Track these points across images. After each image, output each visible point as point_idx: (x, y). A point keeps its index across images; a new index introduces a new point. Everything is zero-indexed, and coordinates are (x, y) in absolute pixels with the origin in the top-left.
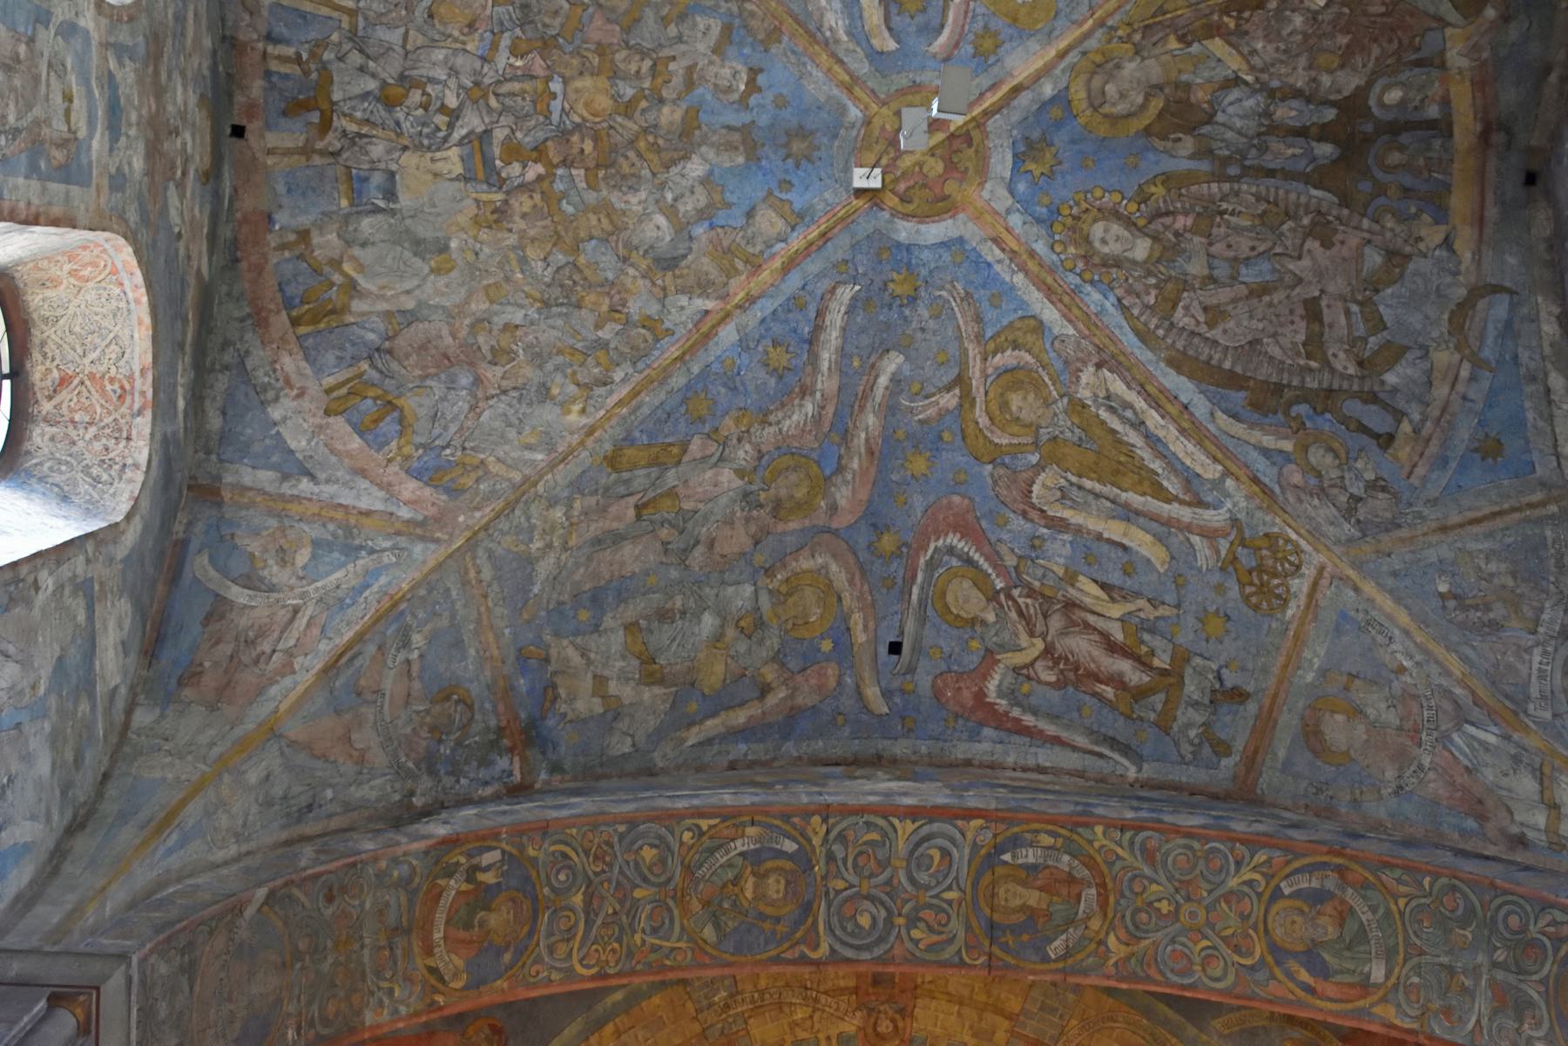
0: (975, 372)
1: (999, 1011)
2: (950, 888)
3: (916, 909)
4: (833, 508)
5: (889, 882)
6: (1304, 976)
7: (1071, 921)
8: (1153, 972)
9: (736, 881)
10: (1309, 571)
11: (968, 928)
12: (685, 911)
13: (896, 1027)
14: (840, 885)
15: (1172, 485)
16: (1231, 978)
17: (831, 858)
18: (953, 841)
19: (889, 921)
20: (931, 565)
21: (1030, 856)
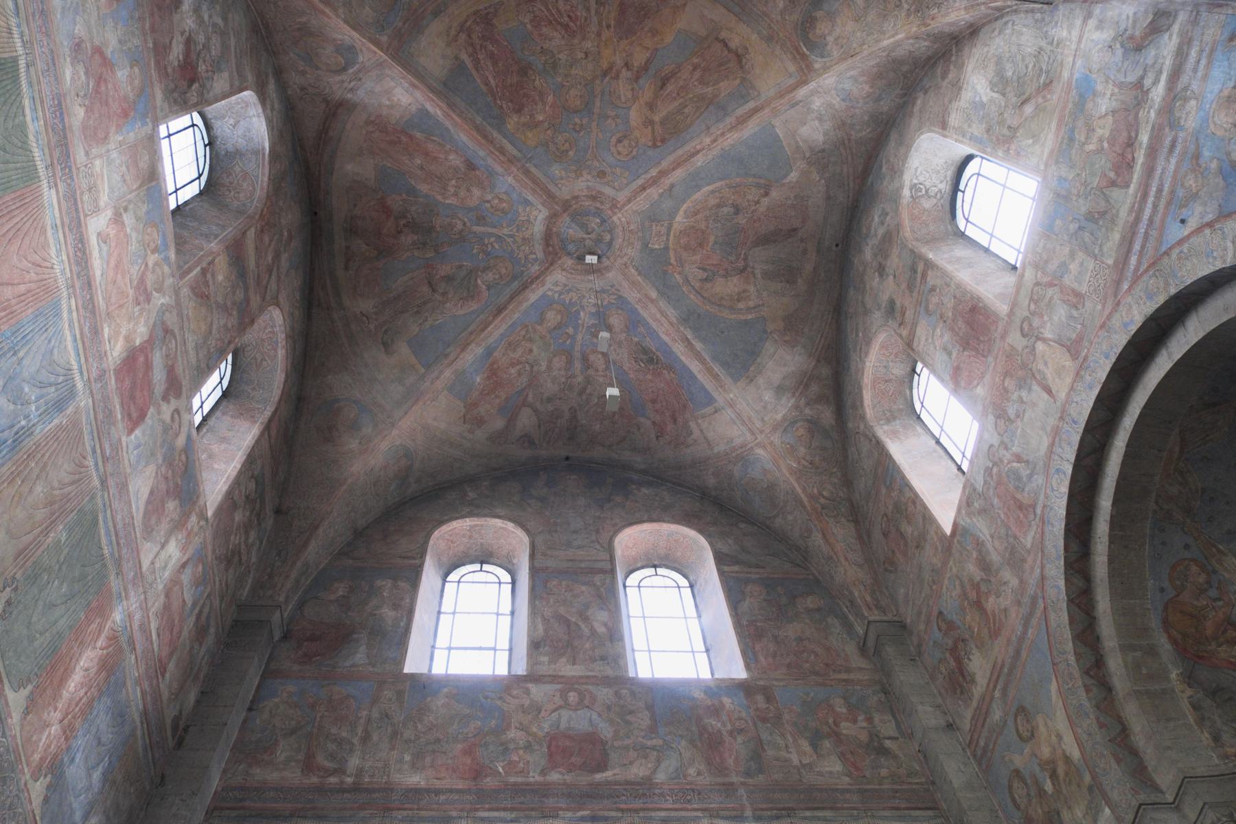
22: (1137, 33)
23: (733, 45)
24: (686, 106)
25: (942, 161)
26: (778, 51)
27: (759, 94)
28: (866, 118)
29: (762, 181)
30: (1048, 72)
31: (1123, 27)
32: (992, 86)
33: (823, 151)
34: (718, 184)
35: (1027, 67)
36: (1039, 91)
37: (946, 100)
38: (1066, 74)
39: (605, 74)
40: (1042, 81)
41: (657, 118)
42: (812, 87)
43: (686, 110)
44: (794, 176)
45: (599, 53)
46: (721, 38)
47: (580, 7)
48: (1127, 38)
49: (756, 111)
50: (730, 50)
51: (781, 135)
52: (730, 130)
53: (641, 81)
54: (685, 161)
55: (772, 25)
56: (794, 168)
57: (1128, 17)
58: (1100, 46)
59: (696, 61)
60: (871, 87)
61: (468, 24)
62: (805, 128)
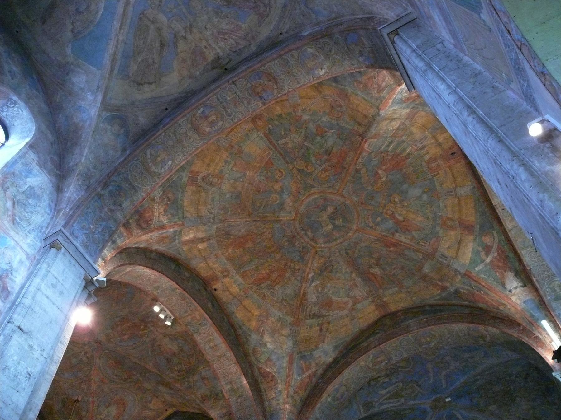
0: (419, 389)
4: (432, 364)
6: (336, 387)
7: (371, 361)
10: (362, 413)
15: (385, 401)
19: (401, 344)
20: (410, 363)
21: (383, 364)
22: (7, 280)
23: (146, 86)
24: (144, 44)
25: (16, 124)
26: (126, 102)
27: (117, 79)
28: (64, 105)
29: (81, 36)
30: (18, 223)
31: (14, 273)
32: (31, 188)
33: (67, 74)
34: (98, 18)
35: (27, 212)
36: (14, 214)
37: (41, 155)
38: (12, 233)
39: (191, 26)
40: (17, 218)
41: (152, 26)
42: (98, 102)
43: (142, 42)
44: (69, 50)
45: (201, 33)
46: (154, 84)
47: (224, 46)
48: (8, 273)
49: (112, 71)
50: (145, 83)
51: (91, 67)
52: (115, 53)
53: (173, 36)
54: (123, 19)
55: (137, 109)
56: (72, 55)
57: (16, 278)
58: (13, 258)
59: (156, 66)
60: (74, 123)
61: (268, 9)
62: (84, 80)
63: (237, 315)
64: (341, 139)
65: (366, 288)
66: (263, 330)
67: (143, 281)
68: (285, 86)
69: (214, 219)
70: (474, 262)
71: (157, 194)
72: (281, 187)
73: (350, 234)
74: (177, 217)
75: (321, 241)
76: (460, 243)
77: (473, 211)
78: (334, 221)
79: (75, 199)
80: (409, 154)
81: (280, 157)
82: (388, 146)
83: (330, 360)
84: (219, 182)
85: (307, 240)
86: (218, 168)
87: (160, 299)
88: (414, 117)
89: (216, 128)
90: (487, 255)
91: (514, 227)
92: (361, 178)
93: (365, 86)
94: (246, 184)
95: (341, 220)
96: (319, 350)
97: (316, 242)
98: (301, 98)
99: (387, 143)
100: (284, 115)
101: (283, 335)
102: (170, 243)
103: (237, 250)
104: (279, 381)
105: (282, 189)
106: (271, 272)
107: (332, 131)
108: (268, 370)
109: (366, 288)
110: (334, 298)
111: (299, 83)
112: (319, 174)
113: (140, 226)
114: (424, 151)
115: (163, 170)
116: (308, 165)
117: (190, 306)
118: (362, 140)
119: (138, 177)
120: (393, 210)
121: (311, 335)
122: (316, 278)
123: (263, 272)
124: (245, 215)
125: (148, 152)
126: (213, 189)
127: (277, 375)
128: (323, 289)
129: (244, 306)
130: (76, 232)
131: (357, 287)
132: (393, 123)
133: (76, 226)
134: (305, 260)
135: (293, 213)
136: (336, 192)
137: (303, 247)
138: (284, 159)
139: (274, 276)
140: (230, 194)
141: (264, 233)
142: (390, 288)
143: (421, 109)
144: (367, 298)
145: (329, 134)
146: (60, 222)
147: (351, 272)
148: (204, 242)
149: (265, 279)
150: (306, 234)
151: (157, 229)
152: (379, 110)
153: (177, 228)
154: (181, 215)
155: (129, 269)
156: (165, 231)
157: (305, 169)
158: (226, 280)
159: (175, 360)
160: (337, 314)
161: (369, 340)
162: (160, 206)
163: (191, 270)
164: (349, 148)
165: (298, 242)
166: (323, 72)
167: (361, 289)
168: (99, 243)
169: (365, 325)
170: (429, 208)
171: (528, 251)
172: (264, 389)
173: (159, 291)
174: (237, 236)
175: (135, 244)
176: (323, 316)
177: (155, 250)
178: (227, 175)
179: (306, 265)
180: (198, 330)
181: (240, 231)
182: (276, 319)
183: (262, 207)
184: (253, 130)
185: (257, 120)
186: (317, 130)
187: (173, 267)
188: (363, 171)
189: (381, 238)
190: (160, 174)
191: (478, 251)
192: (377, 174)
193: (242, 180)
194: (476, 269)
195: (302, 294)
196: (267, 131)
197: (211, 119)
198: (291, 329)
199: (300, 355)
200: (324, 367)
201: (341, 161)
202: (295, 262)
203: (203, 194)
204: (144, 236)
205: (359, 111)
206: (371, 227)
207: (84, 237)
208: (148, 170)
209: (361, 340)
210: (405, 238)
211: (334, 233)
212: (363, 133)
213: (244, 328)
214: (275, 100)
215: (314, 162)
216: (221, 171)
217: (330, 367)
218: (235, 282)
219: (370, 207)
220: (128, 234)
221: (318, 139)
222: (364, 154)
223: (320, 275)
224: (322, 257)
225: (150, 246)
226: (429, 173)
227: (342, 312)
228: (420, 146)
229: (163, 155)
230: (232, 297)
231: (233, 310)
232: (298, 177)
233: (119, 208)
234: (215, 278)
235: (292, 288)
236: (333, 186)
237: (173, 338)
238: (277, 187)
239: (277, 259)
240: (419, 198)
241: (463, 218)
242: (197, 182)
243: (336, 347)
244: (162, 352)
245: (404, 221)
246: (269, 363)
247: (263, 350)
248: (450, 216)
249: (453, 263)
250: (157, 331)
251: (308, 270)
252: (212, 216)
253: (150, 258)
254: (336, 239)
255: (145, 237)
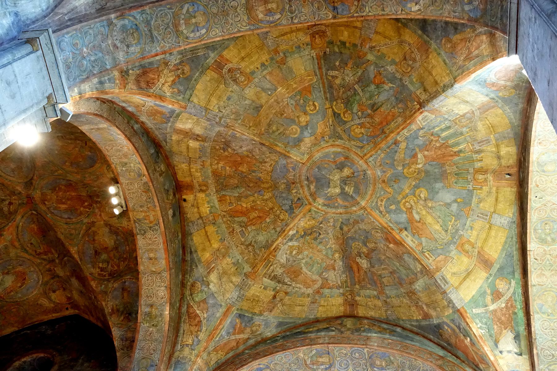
1: (324, 306)
2: (339, 360)
3: (346, 356)
5: (353, 361)
6: (261, 366)
7: (312, 357)
8: (292, 353)
9: (387, 366)
11: (334, 353)
12: (398, 364)
13: (347, 297)
14: (363, 361)
16: (276, 359)
17: (366, 366)
18: (339, 368)
63: (194, 238)
64: (397, 99)
65: (344, 276)
66: (213, 267)
67: (112, 149)
68: (367, 8)
69: (221, 118)
70: (475, 302)
71: (174, 60)
72: (306, 122)
73: (354, 208)
74: (182, 96)
75: (320, 201)
76: (469, 274)
77: (500, 248)
78: (343, 186)
79: (81, 12)
80: (460, 151)
81: (322, 89)
82: (442, 130)
83: (269, 334)
84: (246, 82)
85: (307, 193)
86: (252, 67)
87: (121, 178)
88: (487, 110)
89: (271, 19)
90: (493, 301)
91: (539, 285)
92: (396, 152)
93: (454, 47)
94: (273, 100)
95: (352, 189)
96: (262, 318)
97: (314, 200)
98: (377, 33)
99: (443, 126)
100: (347, 45)
101: (232, 282)
102: (162, 123)
103: (228, 168)
104: (204, 329)
105: (307, 125)
106: (253, 209)
107: (392, 85)
108: (198, 312)
109: (344, 276)
110: (304, 270)
111: (383, 10)
112: (355, 127)
113: (138, 81)
114: (478, 156)
115: (192, 35)
116: (347, 111)
117: (150, 202)
118: (419, 109)
119: (162, 27)
120: (413, 204)
121: (261, 297)
122: (295, 238)
123: (245, 205)
124: (255, 132)
125: (186, 7)
126: (235, 86)
127: (204, 322)
128: (298, 253)
129: (206, 232)
130: (64, 44)
131: (334, 269)
132: (462, 106)
133: (67, 38)
134: (294, 213)
135: (306, 157)
136: (362, 155)
137: (299, 199)
138: (325, 92)
139: (254, 215)
140: (251, 102)
141: (265, 162)
142: (369, 289)
143: (500, 106)
144: (339, 287)
145: (386, 87)
146: (51, 25)
147: (336, 251)
148: (197, 140)
149: (244, 213)
150: (308, 186)
151: (155, 97)
152: (455, 81)
153: (176, 107)
154: (187, 97)
155: (104, 125)
156: (162, 104)
157: (342, 115)
158: (201, 195)
159: (104, 256)
160: (300, 288)
161: (319, 334)
162: (170, 74)
163: (170, 166)
164: (400, 113)
165: (296, 191)
166: (416, 8)
167: (338, 275)
168: (85, 71)
169: (323, 316)
170: (453, 221)
171: (543, 318)
172: (184, 331)
173: (124, 169)
174: (236, 152)
175: (124, 102)
176: (284, 283)
177: (142, 122)
178: (256, 80)
179: (293, 219)
180: (145, 232)
181: (241, 147)
182: (233, 261)
183: (277, 133)
184: (307, 45)
185: (317, 36)
186: (375, 77)
187: (152, 151)
188: (403, 145)
189: (385, 228)
190: (187, 38)
191: (485, 292)
192: (415, 156)
193: (270, 93)
194: (474, 310)
195: (274, 246)
196: (321, 54)
197: (270, 6)
198: (244, 280)
199: (239, 312)
200: (259, 339)
201: (384, 123)
202: (282, 210)
203: (222, 86)
204: (137, 97)
205: (432, 75)
206: (381, 212)
207: (71, 56)
208: (176, 26)
209: (311, 330)
210: (412, 240)
211: (338, 200)
212: (424, 102)
213: (195, 256)
214: (348, 17)
215: (355, 111)
216: (253, 73)
217: (264, 341)
218: (208, 202)
219: (390, 190)
220: (121, 84)
221: (373, 87)
222: (414, 127)
223: (302, 237)
224: (314, 218)
225: (138, 114)
226: (471, 183)
227: (305, 289)
228: (478, 148)
229: (200, 19)
230: (198, 217)
231: (192, 231)
232: (331, 120)
233: (125, 48)
234: (190, 187)
235: (265, 236)
236: (362, 147)
237: (114, 231)
238: (303, 119)
239: (265, 197)
240: (448, 205)
241: (485, 249)
242: (222, 70)
243: (280, 324)
244: (94, 240)
245: (419, 222)
246: (202, 304)
247: (202, 288)
248: (473, 241)
249: (451, 291)
250: (100, 215)
251: (291, 226)
252: (220, 115)
253: (132, 128)
254: (337, 207)
255: (138, 99)
